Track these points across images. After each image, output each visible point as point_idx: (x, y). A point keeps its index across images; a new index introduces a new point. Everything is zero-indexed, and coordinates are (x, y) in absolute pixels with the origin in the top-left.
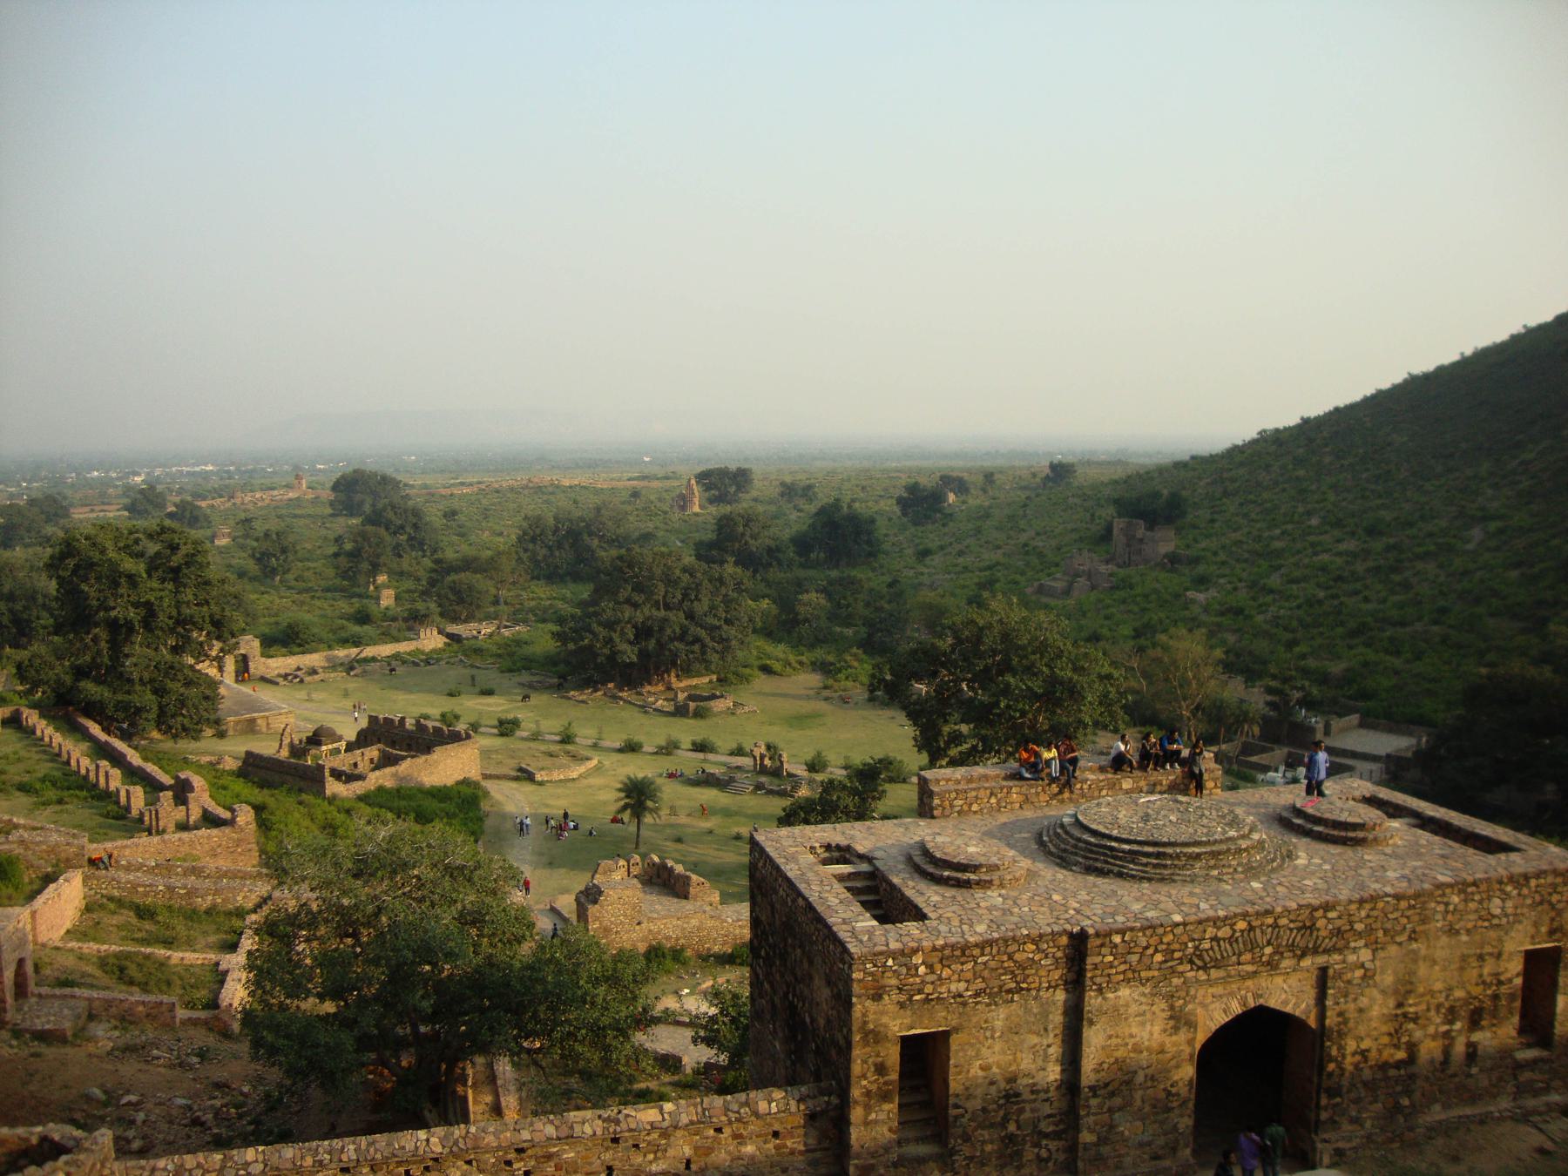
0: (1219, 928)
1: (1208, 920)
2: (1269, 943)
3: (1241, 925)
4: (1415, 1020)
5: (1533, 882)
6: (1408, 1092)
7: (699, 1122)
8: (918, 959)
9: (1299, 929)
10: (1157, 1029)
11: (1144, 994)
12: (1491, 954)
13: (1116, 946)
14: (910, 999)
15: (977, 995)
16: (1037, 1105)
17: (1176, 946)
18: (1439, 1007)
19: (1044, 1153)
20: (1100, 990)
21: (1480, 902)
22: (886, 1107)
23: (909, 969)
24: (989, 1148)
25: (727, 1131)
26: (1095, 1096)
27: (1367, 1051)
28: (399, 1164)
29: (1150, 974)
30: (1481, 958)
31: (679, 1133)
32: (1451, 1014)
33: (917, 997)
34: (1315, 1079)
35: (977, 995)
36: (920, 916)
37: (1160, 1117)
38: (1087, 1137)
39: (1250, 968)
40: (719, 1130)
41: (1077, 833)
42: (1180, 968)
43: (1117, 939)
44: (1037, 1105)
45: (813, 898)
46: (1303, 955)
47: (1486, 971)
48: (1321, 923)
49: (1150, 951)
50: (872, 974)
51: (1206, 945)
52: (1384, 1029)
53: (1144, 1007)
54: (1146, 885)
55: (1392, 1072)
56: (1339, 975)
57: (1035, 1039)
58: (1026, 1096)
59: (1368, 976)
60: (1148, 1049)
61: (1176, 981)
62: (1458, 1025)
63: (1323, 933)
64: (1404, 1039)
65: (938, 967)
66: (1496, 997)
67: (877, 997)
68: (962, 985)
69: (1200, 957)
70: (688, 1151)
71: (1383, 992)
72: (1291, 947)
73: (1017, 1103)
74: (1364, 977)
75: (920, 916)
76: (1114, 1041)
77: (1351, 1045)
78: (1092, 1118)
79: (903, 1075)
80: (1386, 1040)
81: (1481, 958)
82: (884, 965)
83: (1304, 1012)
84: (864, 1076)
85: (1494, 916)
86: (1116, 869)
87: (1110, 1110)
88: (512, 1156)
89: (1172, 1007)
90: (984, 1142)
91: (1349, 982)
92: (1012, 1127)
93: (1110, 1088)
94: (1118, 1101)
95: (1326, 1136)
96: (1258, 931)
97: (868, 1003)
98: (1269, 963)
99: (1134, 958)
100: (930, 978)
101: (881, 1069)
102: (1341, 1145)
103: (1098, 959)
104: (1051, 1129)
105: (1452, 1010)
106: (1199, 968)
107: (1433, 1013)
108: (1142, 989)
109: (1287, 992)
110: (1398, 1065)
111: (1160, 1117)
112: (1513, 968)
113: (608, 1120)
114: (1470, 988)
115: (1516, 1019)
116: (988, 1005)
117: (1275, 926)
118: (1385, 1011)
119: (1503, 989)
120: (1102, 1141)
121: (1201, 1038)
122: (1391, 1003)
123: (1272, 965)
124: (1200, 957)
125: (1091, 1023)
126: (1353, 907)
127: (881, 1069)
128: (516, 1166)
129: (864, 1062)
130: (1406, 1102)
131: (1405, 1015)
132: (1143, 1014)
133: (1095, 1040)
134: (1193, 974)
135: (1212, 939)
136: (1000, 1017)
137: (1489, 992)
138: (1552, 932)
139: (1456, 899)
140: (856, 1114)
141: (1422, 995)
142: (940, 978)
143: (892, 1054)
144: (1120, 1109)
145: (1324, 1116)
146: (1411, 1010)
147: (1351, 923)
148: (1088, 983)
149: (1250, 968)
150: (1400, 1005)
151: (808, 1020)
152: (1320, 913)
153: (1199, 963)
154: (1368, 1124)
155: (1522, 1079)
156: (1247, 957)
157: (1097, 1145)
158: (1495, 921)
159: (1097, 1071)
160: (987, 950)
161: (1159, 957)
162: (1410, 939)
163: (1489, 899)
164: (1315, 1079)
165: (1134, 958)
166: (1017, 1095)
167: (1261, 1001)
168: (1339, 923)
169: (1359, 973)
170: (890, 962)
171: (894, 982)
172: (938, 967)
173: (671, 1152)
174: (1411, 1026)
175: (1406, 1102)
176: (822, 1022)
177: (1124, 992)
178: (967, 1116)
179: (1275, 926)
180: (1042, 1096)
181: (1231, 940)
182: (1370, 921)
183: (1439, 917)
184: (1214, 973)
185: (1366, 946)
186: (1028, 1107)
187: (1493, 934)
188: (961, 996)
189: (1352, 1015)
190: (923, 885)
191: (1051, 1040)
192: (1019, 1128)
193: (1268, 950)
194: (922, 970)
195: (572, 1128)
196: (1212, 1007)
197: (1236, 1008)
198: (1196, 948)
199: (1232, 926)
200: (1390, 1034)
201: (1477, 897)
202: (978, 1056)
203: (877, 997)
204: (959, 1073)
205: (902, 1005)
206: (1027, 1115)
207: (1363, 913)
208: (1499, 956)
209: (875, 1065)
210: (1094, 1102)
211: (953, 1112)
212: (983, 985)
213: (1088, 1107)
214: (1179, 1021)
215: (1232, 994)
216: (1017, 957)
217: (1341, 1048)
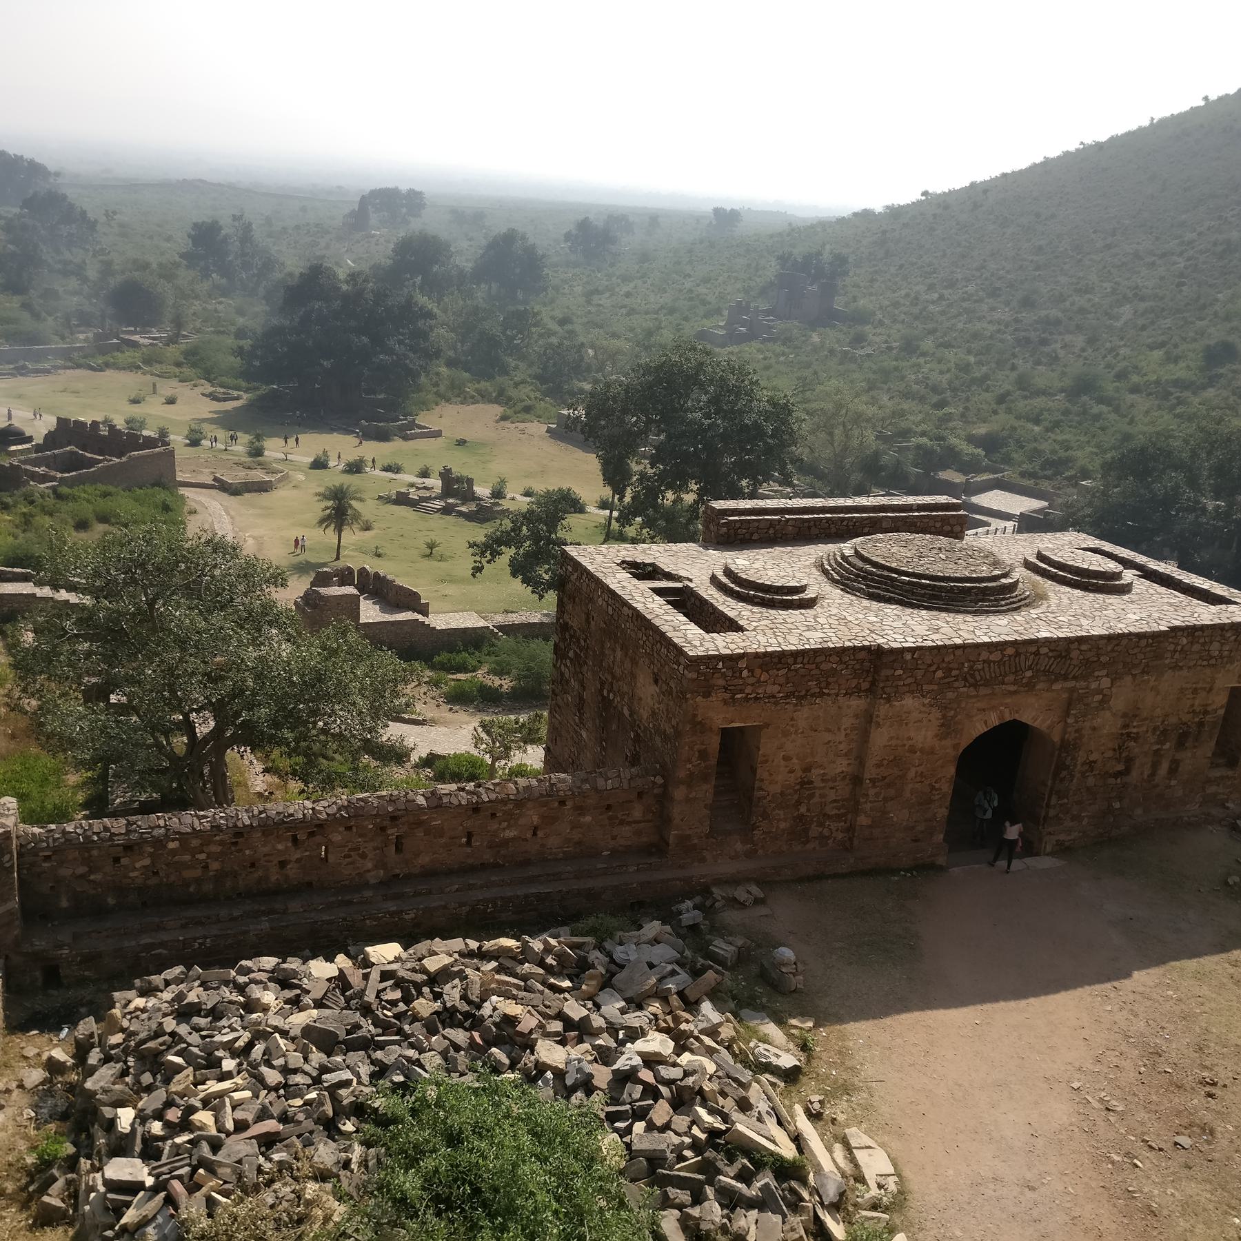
2: (1030, 668)
3: (1010, 651)
4: (1135, 739)
6: (1120, 799)
7: (548, 795)
8: (742, 664)
9: (1055, 658)
10: (930, 734)
11: (924, 705)
12: (1204, 689)
13: (906, 662)
14: (732, 698)
15: (787, 697)
17: (954, 665)
19: (826, 832)
20: (888, 700)
21: (1203, 644)
22: (705, 787)
24: (783, 825)
25: (569, 804)
26: (874, 786)
27: (1095, 762)
28: (288, 829)
30: (1195, 691)
31: (530, 805)
32: (1164, 734)
33: (738, 696)
34: (1049, 783)
35: (787, 697)
36: (740, 629)
39: (1013, 688)
40: (562, 803)
41: (860, 564)
42: (956, 684)
45: (639, 606)
46: (1056, 680)
47: (1197, 702)
48: (1074, 654)
49: (933, 668)
50: (704, 674)
54: (924, 612)
55: (1111, 781)
57: (828, 737)
58: (818, 784)
59: (1105, 700)
60: (922, 750)
61: (950, 695)
62: (1167, 746)
63: (1074, 662)
64: (1124, 755)
65: (758, 671)
66: (1201, 724)
67: (707, 695)
68: (777, 688)
70: (536, 819)
71: (1114, 715)
72: (1046, 672)
74: (1101, 702)
75: (740, 629)
76: (894, 742)
78: (869, 805)
79: (720, 763)
80: (1110, 754)
82: (715, 668)
83: (1049, 727)
84: (689, 761)
85: (1212, 657)
88: (387, 823)
89: (944, 716)
90: (779, 820)
91: (1087, 705)
92: (803, 810)
94: (892, 792)
95: (1051, 829)
96: (1023, 657)
97: (699, 699)
98: (1027, 685)
99: (919, 673)
100: (751, 680)
101: (703, 755)
102: (1062, 837)
103: (889, 672)
104: (835, 812)
105: (1165, 730)
107: (1149, 734)
109: (1034, 711)
110: (1118, 774)
113: (468, 792)
115: (1213, 743)
116: (796, 705)
117: (1037, 654)
119: (1208, 718)
121: (965, 742)
122: (1120, 722)
123: (1030, 686)
124: (973, 676)
127: (703, 755)
128: (389, 832)
129: (691, 748)
130: (1117, 805)
131: (1128, 735)
133: (880, 738)
135: (984, 661)
136: (804, 715)
137: (1197, 720)
139: (1185, 641)
140: (679, 793)
141: (1146, 719)
142: (759, 681)
143: (714, 742)
145: (1052, 813)
146: (1135, 730)
147: (1098, 655)
148: (880, 691)
149: (1013, 688)
150: (1126, 726)
151: (626, 712)
152: (1073, 646)
153: (972, 681)
155: (1208, 791)
156: (1011, 678)
157: (870, 827)
158: (1213, 661)
159: (878, 766)
160: (799, 659)
161: (939, 674)
162: (1143, 672)
163: (1211, 643)
164: (1049, 783)
165: (919, 673)
166: (812, 782)
167: (1017, 717)
168: (1089, 654)
169: (1098, 698)
170: (720, 665)
171: (721, 682)
172: (758, 671)
173: (522, 821)
175: (1117, 805)
176: (645, 714)
177: (909, 702)
178: (768, 798)
179: (1037, 654)
180: (831, 784)
182: (1114, 654)
183: (1169, 655)
184: (983, 691)
185: (1107, 675)
186: (818, 793)
187: (1208, 671)
188: (774, 697)
190: (731, 602)
192: (808, 810)
193: (1029, 674)
194: (745, 673)
195: (440, 798)
197: (994, 720)
198: (971, 668)
201: (1202, 640)
203: (707, 695)
204: (767, 761)
205: (725, 702)
206: (816, 799)
207: (1109, 648)
208: (1211, 689)
211: (757, 794)
212: (792, 689)
214: (947, 728)
215: (993, 708)
216: (823, 666)
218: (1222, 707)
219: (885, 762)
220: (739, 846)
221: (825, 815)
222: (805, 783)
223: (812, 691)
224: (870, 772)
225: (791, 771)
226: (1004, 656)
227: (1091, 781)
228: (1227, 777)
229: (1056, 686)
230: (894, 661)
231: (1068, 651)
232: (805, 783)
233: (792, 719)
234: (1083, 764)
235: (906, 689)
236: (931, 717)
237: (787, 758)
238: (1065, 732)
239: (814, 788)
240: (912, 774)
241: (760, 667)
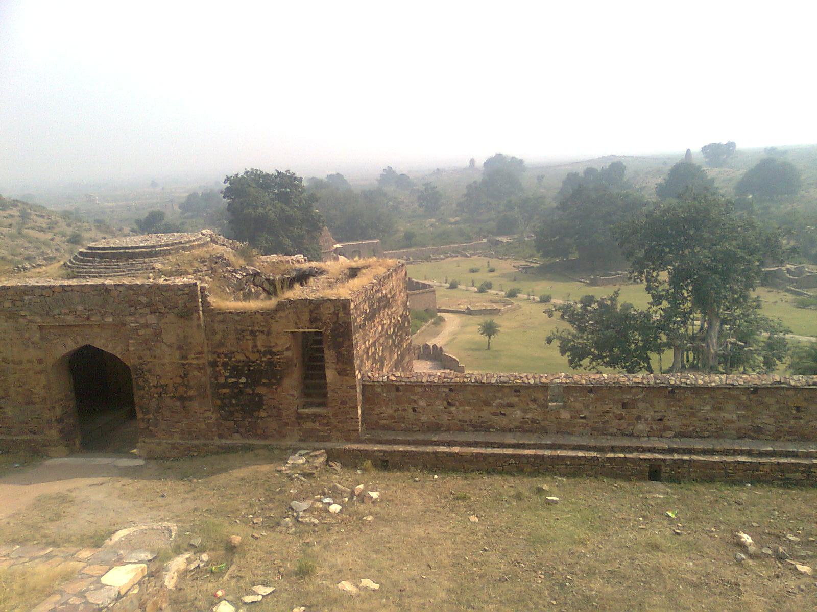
12: (262, 332)
18: (225, 365)
27: (166, 385)
59: (158, 334)
60: (13, 362)
77: (153, 381)
80: (179, 380)
81: (253, 333)
114: (248, 354)
146: (195, 362)
154: (176, 436)
169: (149, 331)
200: (181, 377)
217: (146, 381)
218: (288, 349)
228: (320, 415)
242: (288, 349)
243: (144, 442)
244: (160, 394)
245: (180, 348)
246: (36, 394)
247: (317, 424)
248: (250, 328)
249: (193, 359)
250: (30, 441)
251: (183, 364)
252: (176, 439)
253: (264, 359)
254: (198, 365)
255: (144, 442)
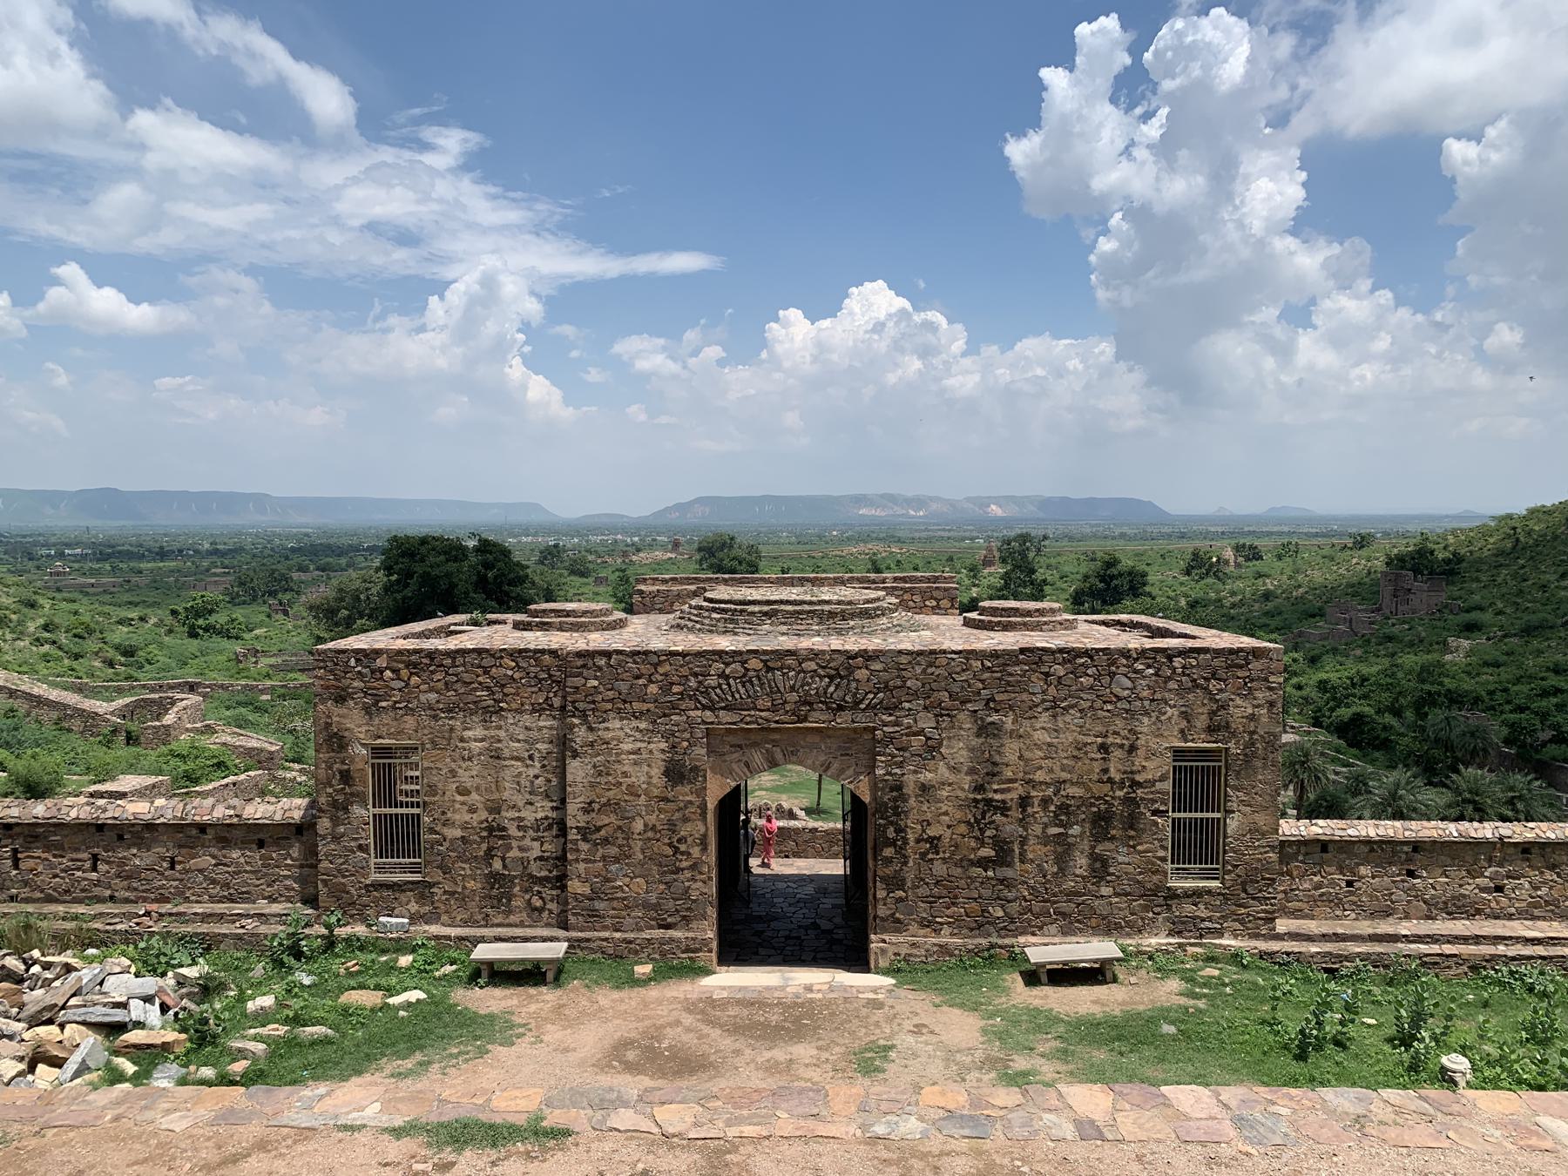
0: (727, 664)
1: (714, 652)
2: (792, 688)
3: (754, 663)
5: (1178, 662)
8: (381, 662)
9: (831, 678)
10: (656, 772)
12: (1122, 746)
13: (600, 669)
16: (527, 842)
18: (1045, 802)
23: (373, 672)
24: (471, 884)
27: (939, 838)
29: (645, 707)
33: (384, 704)
37: (669, 878)
38: (575, 886)
43: (602, 662)
44: (527, 842)
48: (862, 674)
51: (712, 681)
52: (959, 815)
53: (639, 745)
55: (977, 871)
56: (890, 739)
58: (513, 831)
59: (932, 749)
62: (1076, 830)
65: (404, 673)
68: (433, 696)
69: (706, 693)
71: (954, 769)
73: (501, 838)
78: (582, 866)
80: (963, 828)
81: (1104, 748)
85: (1119, 699)
86: (690, 624)
87: (604, 858)
92: (497, 865)
93: (603, 832)
99: (623, 687)
103: (578, 681)
104: (544, 873)
105: (1064, 808)
106: (704, 708)
108: (635, 723)
110: (984, 863)
111: (669, 878)
112: (1156, 768)
118: (960, 793)
120: (595, 895)
122: (967, 782)
124: (706, 693)
125: (575, 755)
126: (904, 659)
131: (988, 802)
132: (638, 752)
134: (699, 713)
138: (1211, 730)
144: (617, 860)
145: (882, 911)
146: (998, 797)
150: (979, 788)
154: (946, 930)
159: (587, 810)
160: (459, 660)
163: (1112, 675)
166: (504, 829)
170: (353, 662)
172: (404, 673)
174: (998, 818)
178: (446, 844)
181: (745, 679)
186: (514, 844)
189: (910, 789)
191: (537, 771)
192: (505, 867)
193: (794, 697)
194: (388, 673)
196: (727, 758)
199: (744, 663)
200: (968, 823)
202: (453, 773)
203: (341, 699)
205: (367, 710)
207: (918, 670)
208: (1133, 749)
209: (341, 772)
210: (584, 846)
213: (578, 850)
218: (1163, 779)
219: (596, 806)
220: (414, 907)
221: (531, 876)
222: (495, 831)
223: (484, 704)
224: (575, 816)
225: (472, 810)
226: (747, 670)
227: (939, 869)
229: (843, 720)
230: (584, 666)
231: (851, 670)
232: (495, 831)
233: (462, 740)
234: (918, 841)
235: (609, 706)
236: (652, 746)
237: (463, 791)
238: (874, 788)
239: (509, 837)
240: (638, 825)
241: (407, 667)
242: (1163, 779)
243: (884, 941)
244: (923, 855)
245: (972, 771)
246: (682, 853)
247: (1202, 906)
248: (1099, 740)
249: (995, 791)
250: (662, 942)
251: (975, 801)
252: (946, 938)
253: (1119, 793)
254: (1004, 802)
255: (884, 941)
